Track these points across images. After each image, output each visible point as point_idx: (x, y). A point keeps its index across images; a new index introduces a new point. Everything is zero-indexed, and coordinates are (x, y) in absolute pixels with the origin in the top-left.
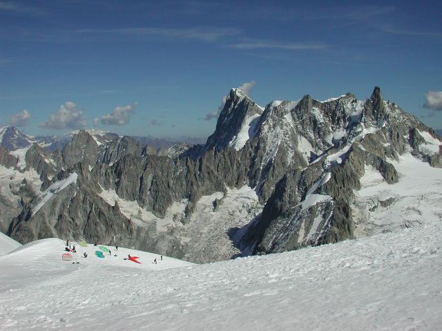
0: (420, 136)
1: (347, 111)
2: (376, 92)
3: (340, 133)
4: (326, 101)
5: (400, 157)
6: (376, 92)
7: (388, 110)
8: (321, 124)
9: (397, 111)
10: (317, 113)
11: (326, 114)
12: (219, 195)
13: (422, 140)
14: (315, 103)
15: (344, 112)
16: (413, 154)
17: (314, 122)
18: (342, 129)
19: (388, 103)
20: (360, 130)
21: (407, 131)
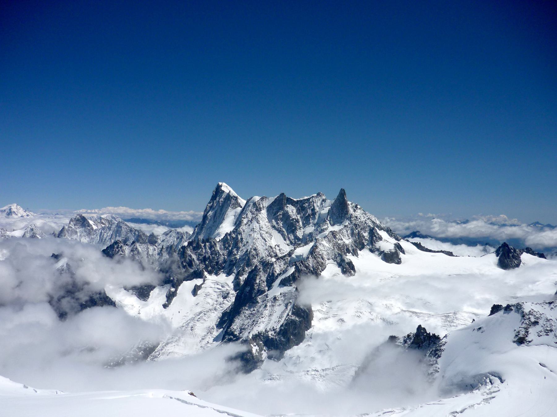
0: (378, 234)
1: (317, 209)
2: (342, 193)
3: (310, 229)
4: (299, 199)
5: (359, 252)
6: (342, 193)
7: (351, 211)
8: (293, 219)
9: (359, 211)
10: (291, 210)
11: (299, 212)
12: (199, 282)
13: (381, 238)
14: (290, 201)
15: (313, 210)
16: (372, 251)
17: (286, 217)
18: (311, 224)
19: (352, 204)
20: (326, 227)
21: (368, 229)
